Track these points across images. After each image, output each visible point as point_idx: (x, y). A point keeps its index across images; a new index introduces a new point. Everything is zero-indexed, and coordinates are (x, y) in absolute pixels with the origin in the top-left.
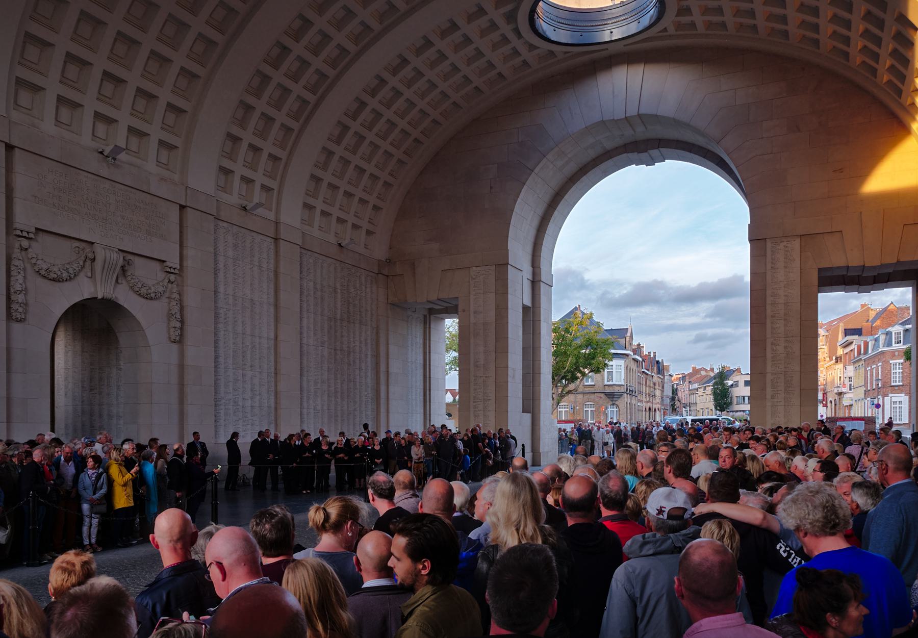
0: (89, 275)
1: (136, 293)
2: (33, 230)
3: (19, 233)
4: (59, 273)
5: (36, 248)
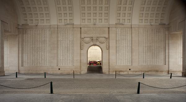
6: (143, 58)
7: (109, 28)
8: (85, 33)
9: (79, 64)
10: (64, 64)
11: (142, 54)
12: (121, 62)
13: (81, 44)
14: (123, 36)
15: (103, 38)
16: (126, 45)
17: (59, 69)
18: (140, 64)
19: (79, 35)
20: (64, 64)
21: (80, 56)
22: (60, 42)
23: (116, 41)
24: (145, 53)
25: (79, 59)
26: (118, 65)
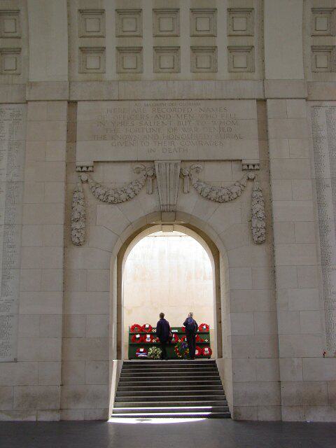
0: (151, 191)
1: (208, 198)
2: (92, 164)
3: (80, 169)
4: (116, 195)
7: (262, 102)
8: (104, 138)
13: (69, 208)
15: (228, 165)
19: (62, 145)
21: (66, 287)
23: (318, 184)
25: (59, 311)
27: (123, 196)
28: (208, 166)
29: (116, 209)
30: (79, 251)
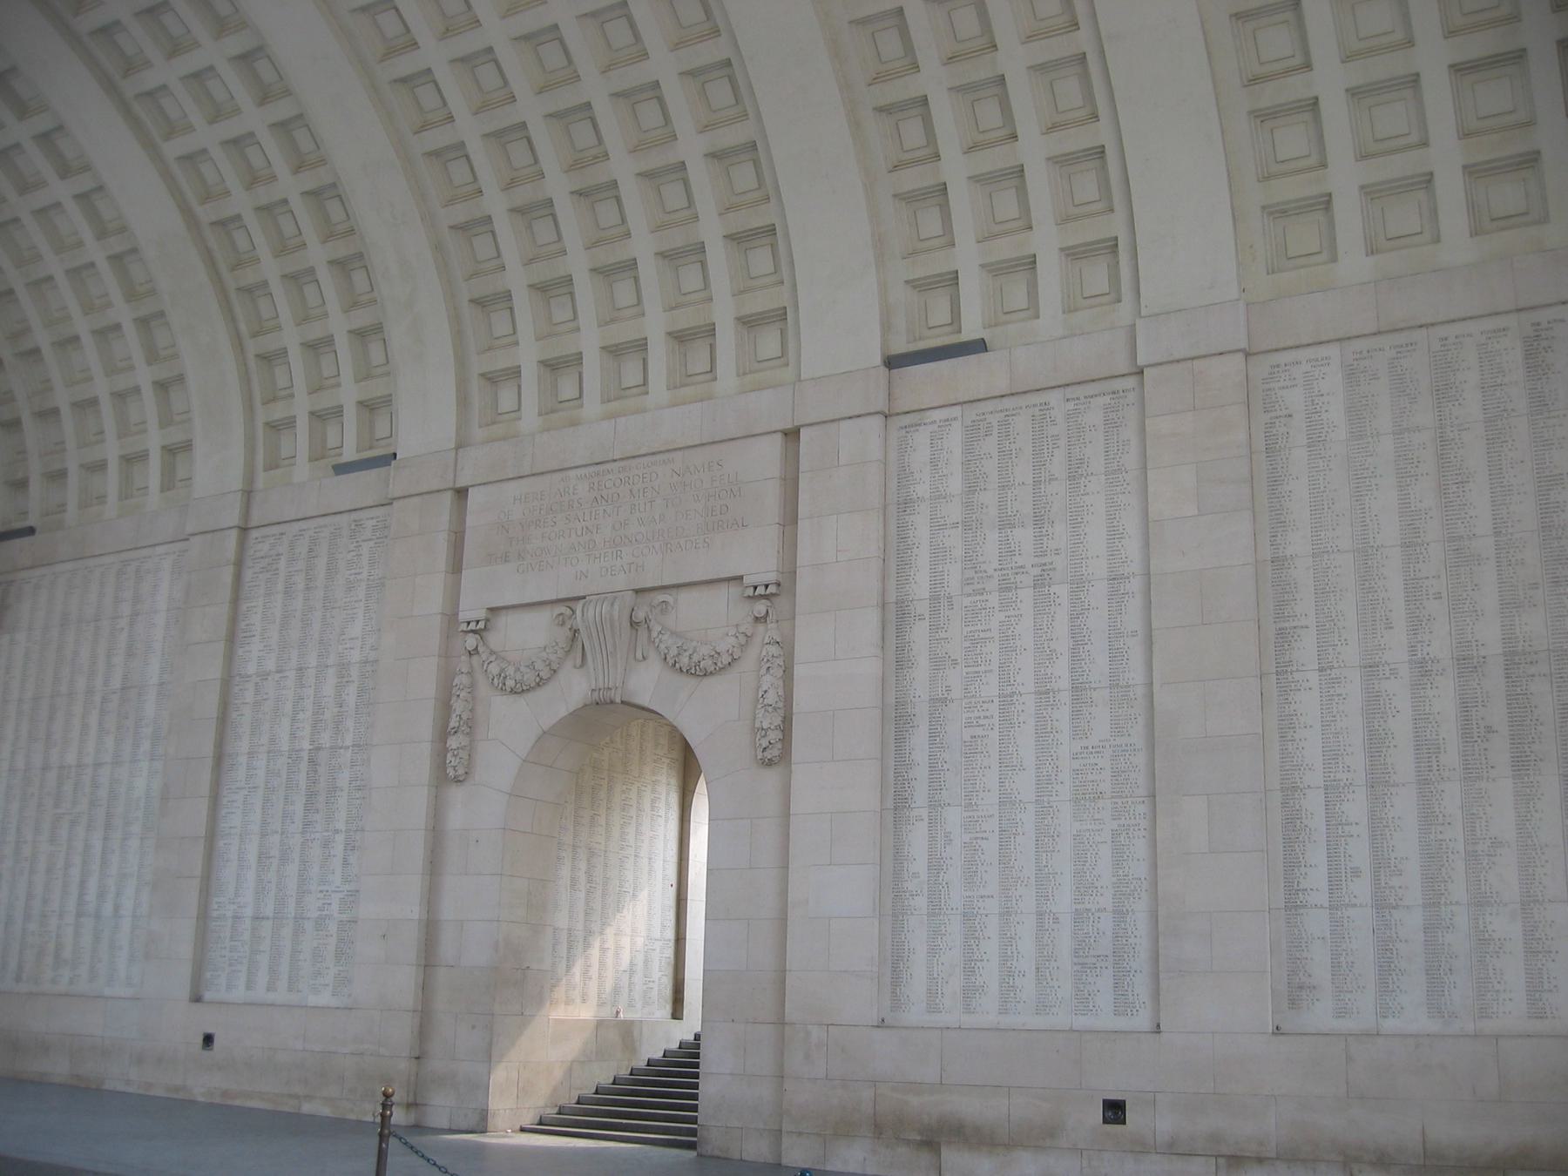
0: (579, 661)
4: (518, 677)
5: (494, 639)
6: (1383, 905)
9: (403, 983)
10: (262, 978)
11: (1356, 807)
12: (970, 969)
14: (1006, 523)
16: (1061, 670)
17: (208, 1040)
18: (1320, 1015)
20: (262, 978)
22: (249, 696)
24: (1404, 805)
26: (915, 1013)
27: (530, 677)
28: (685, 597)
29: (521, 703)
30: (456, 794)
